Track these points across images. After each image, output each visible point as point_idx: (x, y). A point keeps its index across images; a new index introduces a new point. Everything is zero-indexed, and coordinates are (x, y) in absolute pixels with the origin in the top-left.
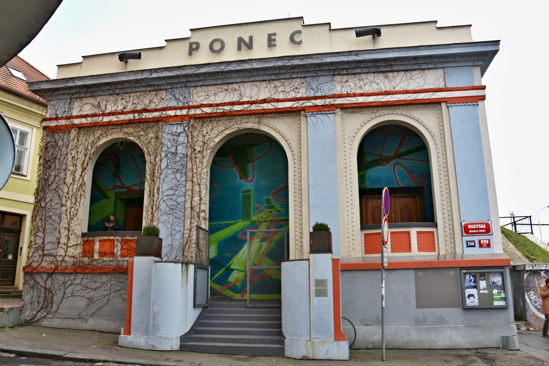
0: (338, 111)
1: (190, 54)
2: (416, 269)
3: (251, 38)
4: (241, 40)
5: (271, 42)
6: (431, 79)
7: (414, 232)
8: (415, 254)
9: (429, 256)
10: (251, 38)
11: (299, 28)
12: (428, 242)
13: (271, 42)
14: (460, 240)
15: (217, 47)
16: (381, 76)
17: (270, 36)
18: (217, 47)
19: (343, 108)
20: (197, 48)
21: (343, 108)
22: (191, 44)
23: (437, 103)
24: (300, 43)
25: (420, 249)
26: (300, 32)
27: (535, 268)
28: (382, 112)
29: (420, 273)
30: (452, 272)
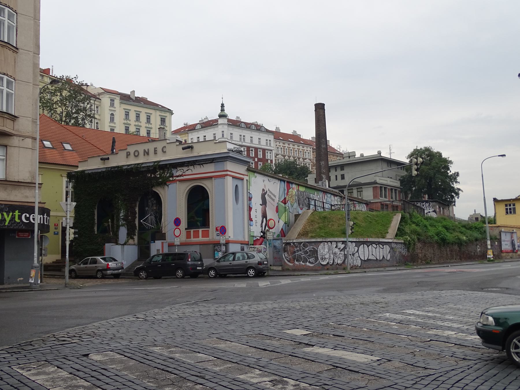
0: (178, 182)
1: (127, 157)
2: (200, 244)
3: (148, 149)
4: (145, 151)
5: (155, 152)
6: (209, 168)
7: (200, 230)
8: (201, 239)
9: (206, 239)
10: (148, 149)
11: (165, 144)
12: (206, 234)
13: (155, 152)
14: (215, 233)
15: (136, 154)
16: (192, 167)
17: (155, 148)
18: (136, 154)
19: (180, 181)
20: (130, 154)
21: (180, 181)
22: (127, 153)
23: (211, 178)
24: (165, 152)
25: (202, 237)
26: (165, 147)
28: (193, 182)
29: (201, 246)
30: (211, 246)
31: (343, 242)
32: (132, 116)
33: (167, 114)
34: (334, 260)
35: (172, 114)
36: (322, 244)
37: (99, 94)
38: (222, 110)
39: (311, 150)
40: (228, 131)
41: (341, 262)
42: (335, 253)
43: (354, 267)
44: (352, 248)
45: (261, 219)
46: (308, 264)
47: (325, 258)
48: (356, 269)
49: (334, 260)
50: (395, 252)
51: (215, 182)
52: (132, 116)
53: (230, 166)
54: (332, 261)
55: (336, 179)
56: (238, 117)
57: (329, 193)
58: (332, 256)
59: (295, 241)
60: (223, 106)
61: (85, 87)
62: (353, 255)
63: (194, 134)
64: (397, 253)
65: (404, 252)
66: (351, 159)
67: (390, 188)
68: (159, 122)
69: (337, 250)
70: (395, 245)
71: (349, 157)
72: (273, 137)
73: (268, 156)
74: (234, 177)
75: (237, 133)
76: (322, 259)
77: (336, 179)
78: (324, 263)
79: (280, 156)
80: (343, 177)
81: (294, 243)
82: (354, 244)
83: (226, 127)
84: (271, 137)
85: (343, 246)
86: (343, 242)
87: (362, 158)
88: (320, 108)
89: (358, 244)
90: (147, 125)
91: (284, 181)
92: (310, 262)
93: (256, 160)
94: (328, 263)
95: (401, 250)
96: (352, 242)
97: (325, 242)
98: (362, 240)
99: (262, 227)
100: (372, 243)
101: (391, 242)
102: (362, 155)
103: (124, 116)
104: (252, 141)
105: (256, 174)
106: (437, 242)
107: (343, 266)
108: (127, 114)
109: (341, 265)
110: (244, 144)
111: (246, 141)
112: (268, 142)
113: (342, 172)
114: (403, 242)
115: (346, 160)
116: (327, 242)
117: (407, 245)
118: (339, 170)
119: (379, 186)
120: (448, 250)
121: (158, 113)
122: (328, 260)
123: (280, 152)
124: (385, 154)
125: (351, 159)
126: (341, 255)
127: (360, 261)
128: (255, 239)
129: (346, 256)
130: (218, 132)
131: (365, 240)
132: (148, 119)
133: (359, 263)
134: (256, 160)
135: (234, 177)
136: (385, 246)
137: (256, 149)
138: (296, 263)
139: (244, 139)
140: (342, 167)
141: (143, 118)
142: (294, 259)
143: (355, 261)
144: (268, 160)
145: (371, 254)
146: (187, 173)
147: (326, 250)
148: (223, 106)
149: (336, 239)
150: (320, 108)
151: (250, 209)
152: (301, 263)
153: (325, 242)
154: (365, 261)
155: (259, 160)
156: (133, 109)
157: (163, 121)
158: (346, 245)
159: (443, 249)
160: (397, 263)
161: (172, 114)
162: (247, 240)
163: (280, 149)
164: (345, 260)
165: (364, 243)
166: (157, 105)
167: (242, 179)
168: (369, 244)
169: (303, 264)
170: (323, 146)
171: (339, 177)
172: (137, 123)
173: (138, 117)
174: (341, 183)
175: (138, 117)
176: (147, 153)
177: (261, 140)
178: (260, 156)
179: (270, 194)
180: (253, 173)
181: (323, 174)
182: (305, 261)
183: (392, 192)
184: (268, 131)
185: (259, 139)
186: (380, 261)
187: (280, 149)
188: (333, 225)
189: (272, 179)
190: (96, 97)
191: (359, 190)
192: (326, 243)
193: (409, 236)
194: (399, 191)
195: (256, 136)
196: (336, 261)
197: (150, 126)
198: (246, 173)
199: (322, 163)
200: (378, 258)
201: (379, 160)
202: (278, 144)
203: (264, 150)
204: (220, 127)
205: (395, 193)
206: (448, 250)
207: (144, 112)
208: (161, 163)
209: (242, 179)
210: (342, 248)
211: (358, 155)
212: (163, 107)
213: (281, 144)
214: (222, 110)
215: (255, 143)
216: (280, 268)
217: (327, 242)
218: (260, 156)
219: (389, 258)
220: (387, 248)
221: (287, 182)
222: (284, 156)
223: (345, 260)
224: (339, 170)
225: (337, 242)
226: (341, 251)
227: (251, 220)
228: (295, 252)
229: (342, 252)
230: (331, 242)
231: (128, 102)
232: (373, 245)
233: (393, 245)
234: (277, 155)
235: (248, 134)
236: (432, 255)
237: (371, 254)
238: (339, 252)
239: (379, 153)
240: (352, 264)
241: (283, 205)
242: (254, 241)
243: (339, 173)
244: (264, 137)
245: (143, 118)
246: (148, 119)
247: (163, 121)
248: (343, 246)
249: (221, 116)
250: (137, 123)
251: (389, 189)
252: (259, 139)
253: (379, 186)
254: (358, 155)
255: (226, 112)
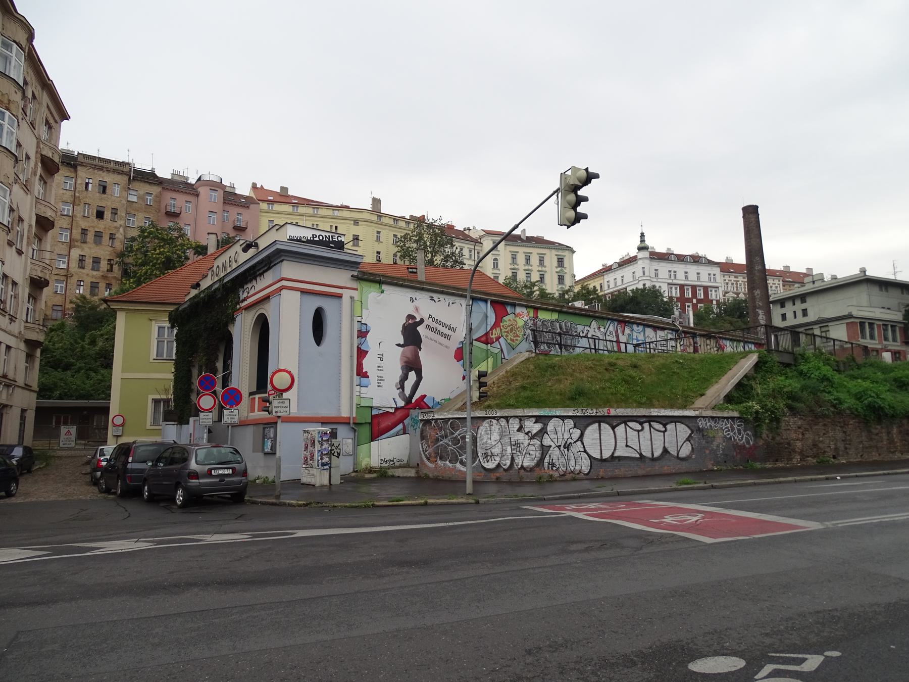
23: (267, 298)
27: (425, 418)
31: (538, 419)
32: (521, 259)
33: (566, 253)
34: (513, 459)
35: (573, 252)
36: (486, 424)
37: (481, 237)
38: (642, 241)
39: (781, 283)
40: (650, 267)
41: (533, 463)
42: (517, 444)
43: (568, 477)
44: (561, 431)
45: (399, 373)
46: (458, 465)
47: (492, 455)
48: (574, 479)
49: (513, 459)
50: (709, 440)
51: (273, 301)
52: (521, 259)
53: (288, 269)
54: (508, 462)
55: (795, 317)
56: (668, 249)
57: (638, 324)
58: (509, 449)
59: (436, 417)
60: (642, 235)
61: (467, 232)
62: (567, 446)
63: (610, 275)
64: (718, 440)
65: (743, 438)
66: (817, 284)
67: (881, 323)
68: (555, 263)
69: (521, 436)
70: (712, 423)
71: (814, 282)
72: (718, 269)
73: (713, 295)
74: (304, 292)
75: (664, 268)
76: (486, 456)
77: (795, 317)
78: (490, 465)
79: (731, 294)
80: (805, 313)
81: (437, 420)
82: (570, 423)
83: (647, 261)
84: (717, 271)
85: (537, 427)
86: (538, 419)
87: (834, 281)
88: (751, 214)
89: (582, 423)
90: (540, 269)
91: (486, 301)
92: (462, 463)
93: (694, 301)
94: (499, 466)
95: (731, 433)
96: (563, 418)
97: (494, 418)
98: (591, 412)
99: (402, 387)
100: (625, 420)
101: (696, 417)
102: (834, 278)
103: (510, 261)
104: (686, 277)
105: (384, 287)
106: (854, 414)
107: (537, 473)
108: (514, 258)
109: (531, 470)
110: (675, 282)
111: (689, 279)
112: (712, 276)
113: (804, 306)
114: (736, 414)
115: (809, 288)
116: (498, 418)
117: (753, 422)
118: (798, 302)
119: (858, 321)
120: (895, 430)
121: (554, 252)
122: (498, 459)
123: (730, 289)
124: (871, 273)
125: (817, 284)
126: (531, 448)
127: (587, 462)
128: (375, 412)
129: (545, 449)
130: (637, 268)
131: (604, 412)
132: (541, 260)
133: (584, 465)
134: (694, 301)
135: (304, 292)
136: (668, 427)
137: (694, 288)
138: (439, 462)
139: (675, 276)
140: (803, 298)
141: (535, 260)
142: (437, 454)
143: (572, 462)
144: (712, 300)
145: (621, 443)
146: (252, 292)
147: (495, 436)
148: (642, 235)
149: (519, 412)
150: (751, 214)
151: (362, 354)
152: (448, 462)
153: (494, 418)
154: (602, 460)
155: (699, 301)
156: (521, 251)
157: (560, 262)
158: (546, 425)
159: (876, 429)
160: (717, 463)
161: (573, 252)
162: (345, 413)
163: (730, 285)
164: (542, 460)
165: (599, 420)
166: (553, 243)
167: (340, 296)
168: (614, 422)
169: (450, 465)
170: (758, 267)
171: (799, 314)
172: (526, 267)
173: (528, 259)
174: (801, 320)
175: (528, 259)
176: (224, 267)
177: (689, 274)
178: (701, 294)
179: (434, 325)
180: (377, 285)
181: (760, 308)
182: (454, 460)
183: (886, 330)
184: (711, 263)
185: (686, 273)
186: (653, 459)
187: (730, 285)
188: (559, 381)
189: (442, 297)
190: (476, 242)
191: (824, 329)
192: (494, 422)
193: (759, 402)
194: (900, 328)
195: (693, 270)
196: (519, 461)
197: (544, 269)
198: (354, 284)
199: (757, 292)
200: (647, 453)
201: (864, 281)
202: (727, 278)
203: (706, 289)
204: (640, 262)
205: (894, 331)
206: (895, 430)
207: (535, 252)
208: (225, 281)
209: (340, 296)
210: (534, 432)
211: (827, 278)
212: (560, 244)
213: (732, 278)
214: (642, 241)
215: (693, 279)
216: (412, 473)
217: (498, 418)
218: (701, 294)
219: (686, 450)
220: (683, 431)
221: (492, 302)
222: (738, 294)
223: (542, 460)
224: (798, 302)
225: (521, 419)
226: (532, 438)
227: (361, 374)
228: (438, 440)
229: (536, 442)
230: (507, 418)
231: (515, 243)
232: (630, 424)
233: (701, 424)
234: (726, 293)
235: (680, 269)
236: (841, 446)
237: (621, 443)
238: (527, 442)
239: (863, 271)
240: (562, 469)
241: (483, 346)
242: (373, 417)
243: (799, 306)
244: (705, 271)
245: (535, 260)
246: (541, 260)
247: (560, 262)
248: (537, 427)
249: (640, 249)
250: (526, 267)
251: (879, 326)
252: (686, 273)
253: (858, 321)
254: (827, 278)
255: (649, 242)
